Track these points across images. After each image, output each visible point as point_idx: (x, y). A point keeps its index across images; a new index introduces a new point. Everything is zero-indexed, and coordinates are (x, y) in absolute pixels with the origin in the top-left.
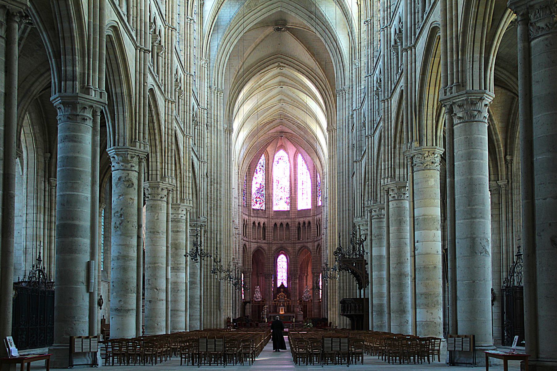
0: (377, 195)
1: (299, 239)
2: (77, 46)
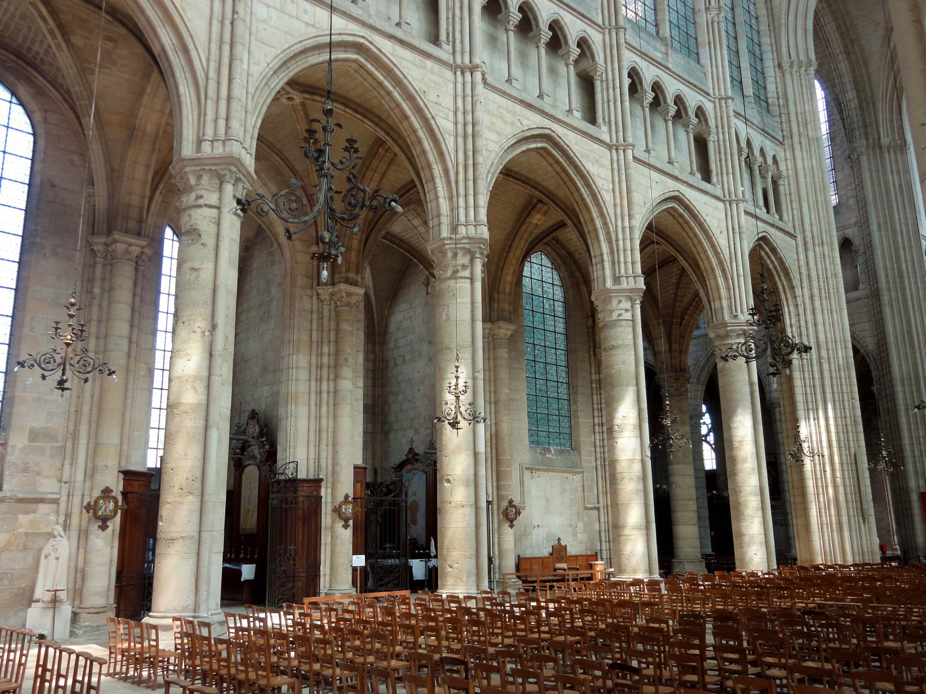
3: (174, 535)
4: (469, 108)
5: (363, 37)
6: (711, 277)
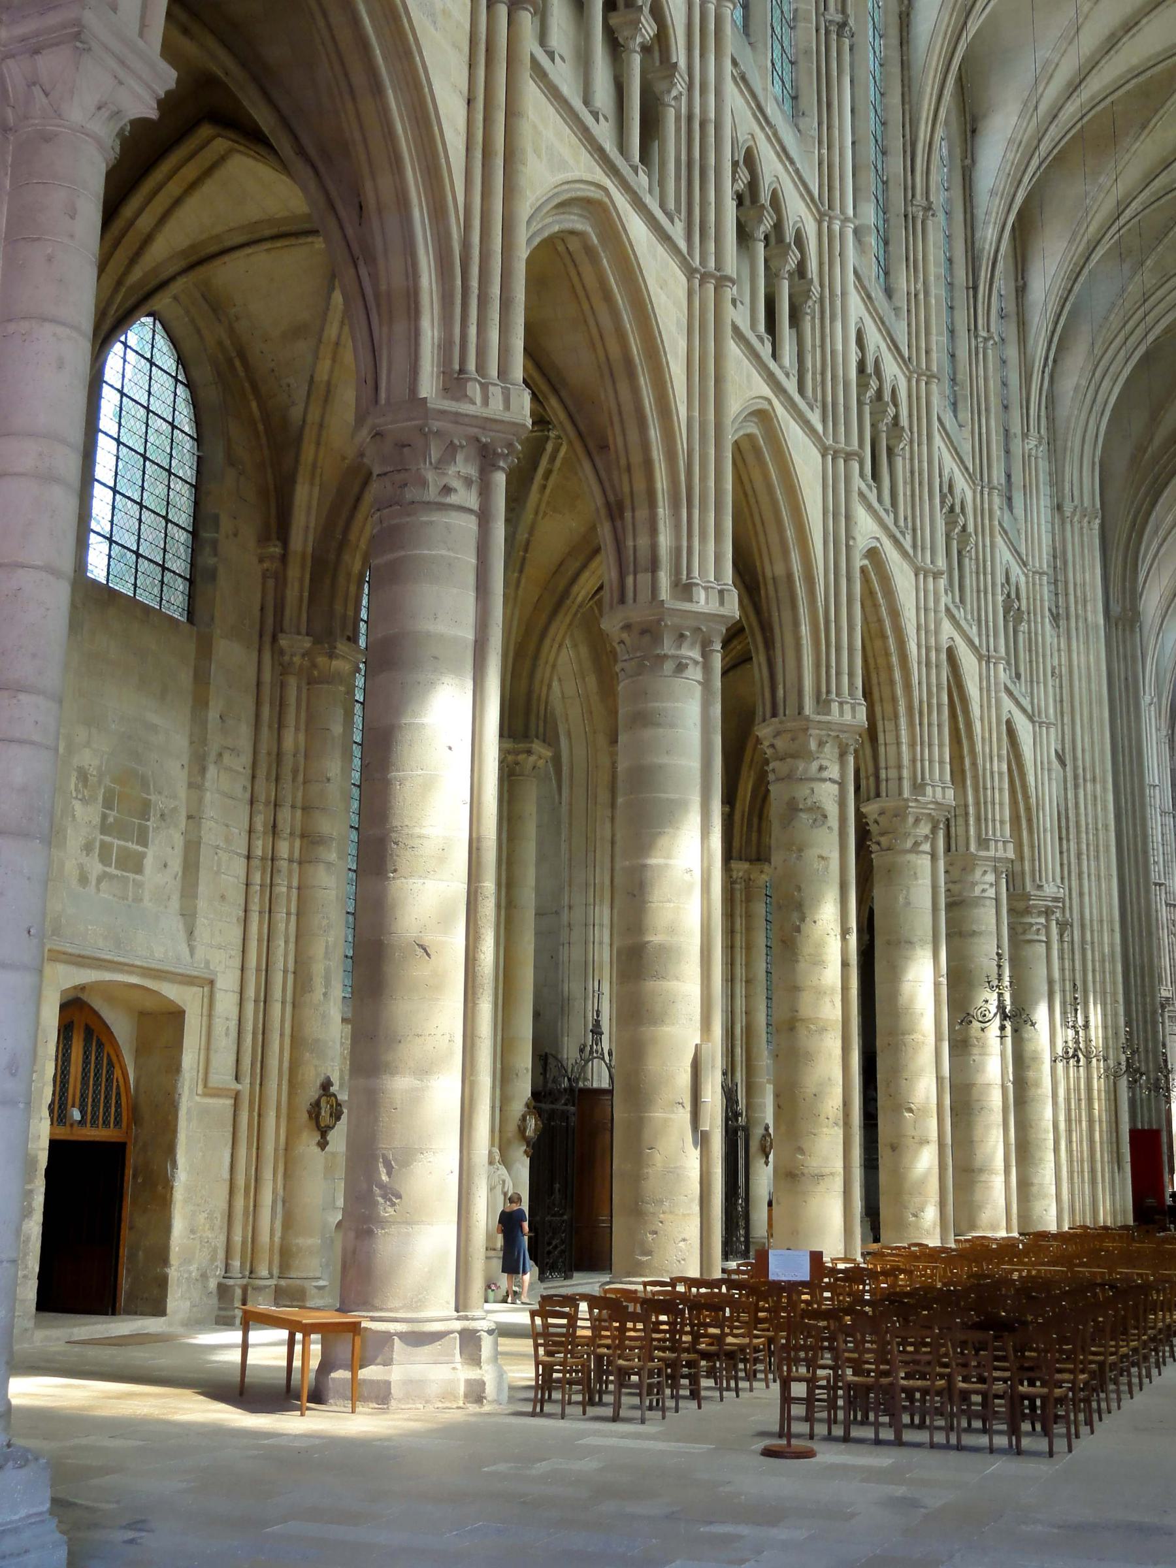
2: (661, 483)
3: (827, 1171)
4: (932, 627)
5: (877, 539)
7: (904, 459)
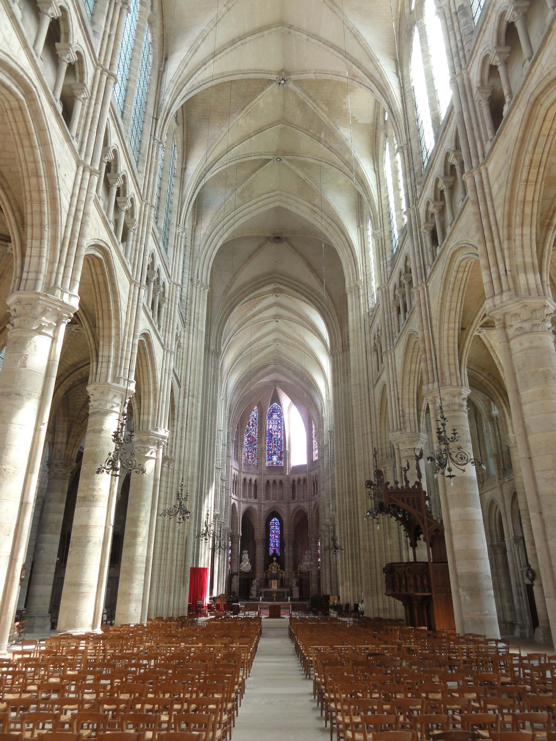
0: (442, 374)
1: (293, 498)
6: (146, 397)
7: (83, 105)
